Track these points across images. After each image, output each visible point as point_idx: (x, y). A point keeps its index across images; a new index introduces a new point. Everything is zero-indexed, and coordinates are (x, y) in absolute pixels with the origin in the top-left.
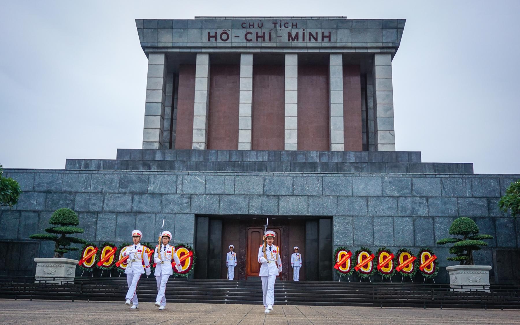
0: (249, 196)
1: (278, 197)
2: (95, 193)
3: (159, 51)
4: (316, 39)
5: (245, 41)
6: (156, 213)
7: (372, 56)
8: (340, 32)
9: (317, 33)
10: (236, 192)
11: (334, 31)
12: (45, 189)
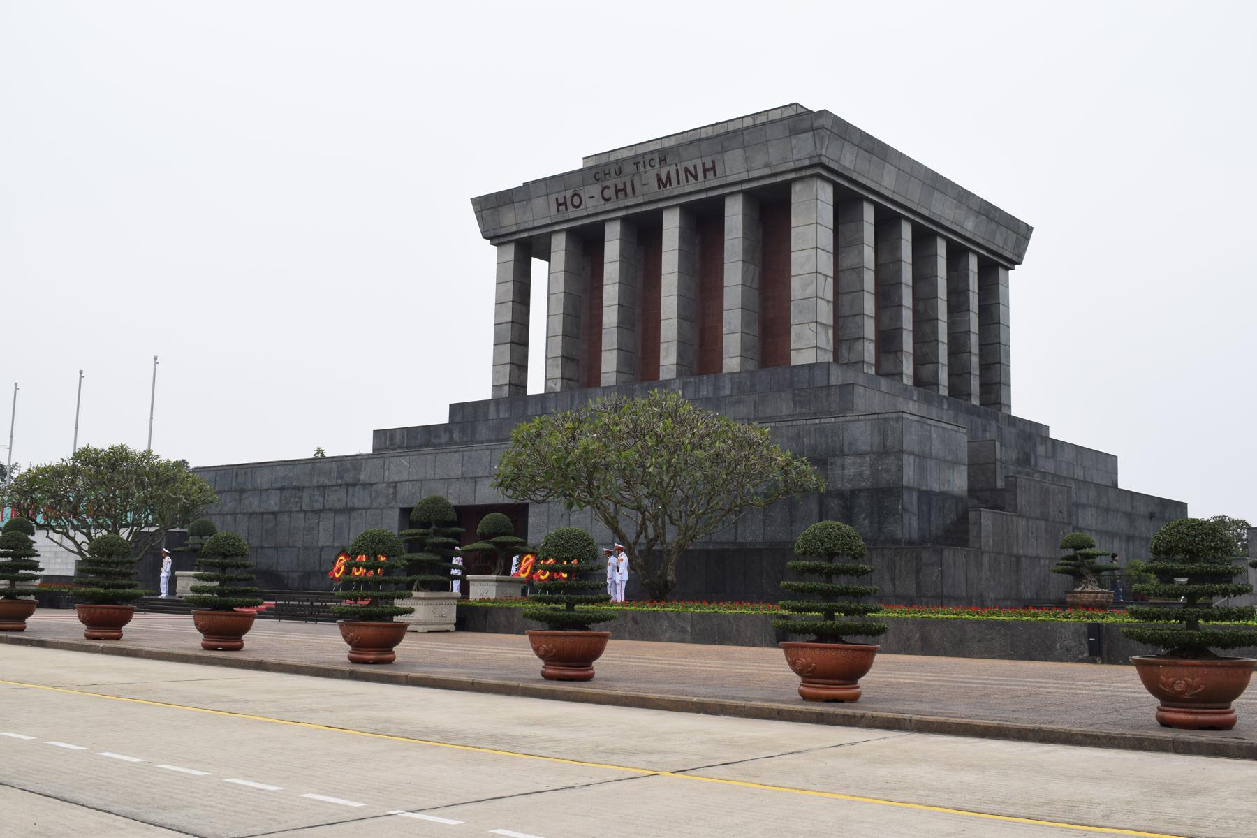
1: (475, 479)
2: (318, 487)
3: (506, 239)
4: (696, 177)
5: (602, 202)
6: (366, 509)
7: (787, 186)
8: (729, 156)
10: (437, 477)
11: (719, 156)
12: (278, 485)
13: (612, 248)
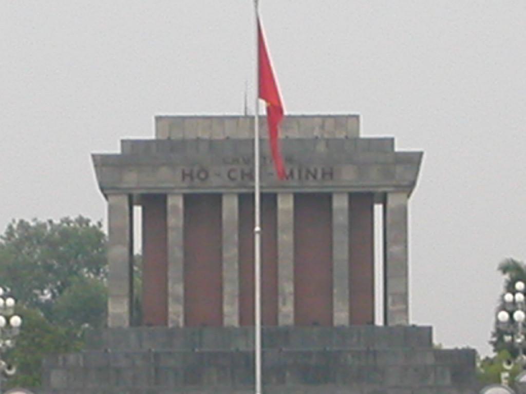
4: (315, 177)
9: (316, 170)
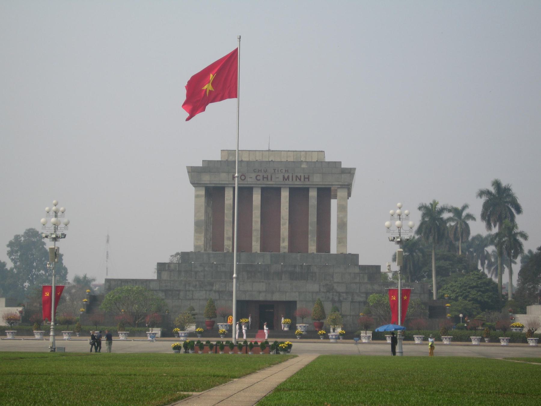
0: (260, 292)
2: (189, 291)
4: (300, 180)
13: (257, 198)
